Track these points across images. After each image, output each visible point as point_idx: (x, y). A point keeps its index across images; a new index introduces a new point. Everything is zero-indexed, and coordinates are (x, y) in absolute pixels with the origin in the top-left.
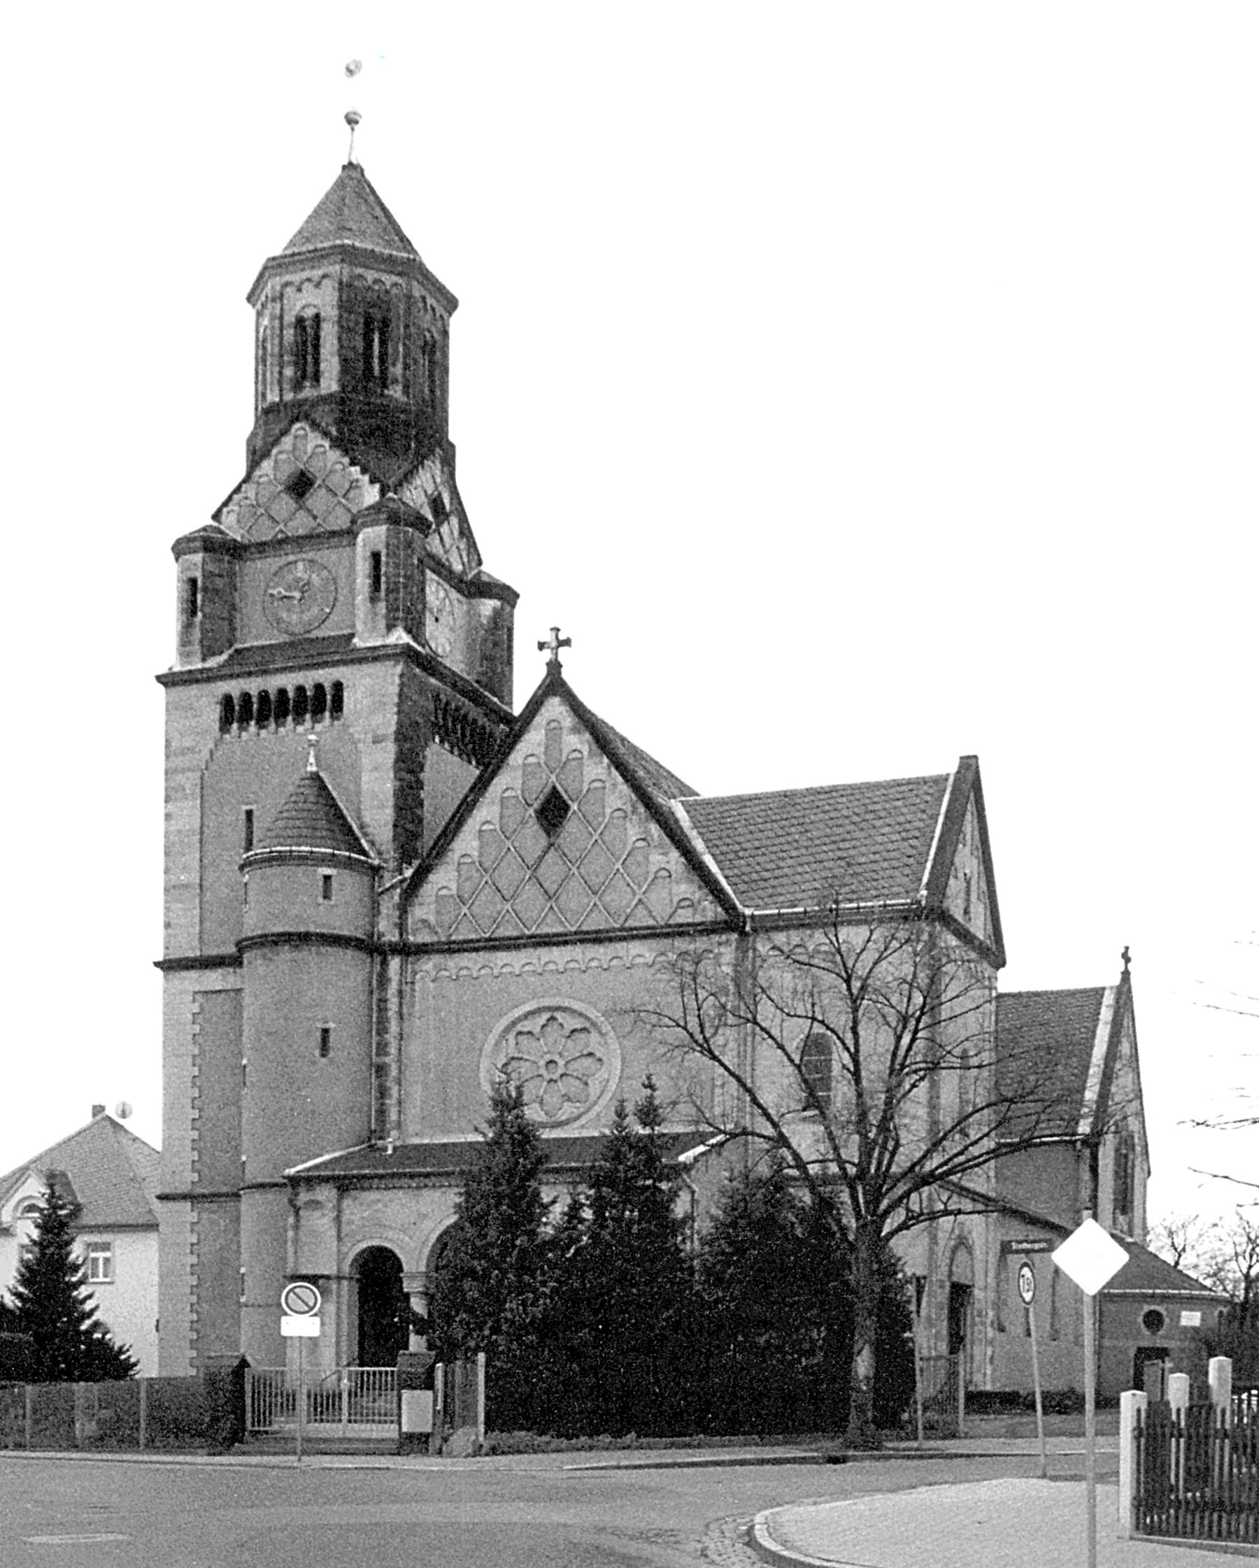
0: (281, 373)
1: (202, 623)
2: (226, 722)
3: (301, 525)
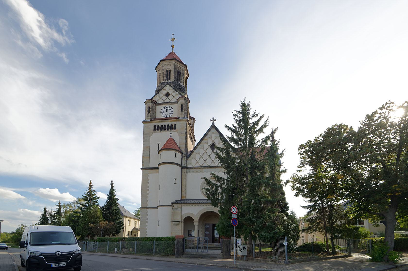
0: (164, 78)
1: (151, 114)
2: (155, 130)
3: (167, 101)
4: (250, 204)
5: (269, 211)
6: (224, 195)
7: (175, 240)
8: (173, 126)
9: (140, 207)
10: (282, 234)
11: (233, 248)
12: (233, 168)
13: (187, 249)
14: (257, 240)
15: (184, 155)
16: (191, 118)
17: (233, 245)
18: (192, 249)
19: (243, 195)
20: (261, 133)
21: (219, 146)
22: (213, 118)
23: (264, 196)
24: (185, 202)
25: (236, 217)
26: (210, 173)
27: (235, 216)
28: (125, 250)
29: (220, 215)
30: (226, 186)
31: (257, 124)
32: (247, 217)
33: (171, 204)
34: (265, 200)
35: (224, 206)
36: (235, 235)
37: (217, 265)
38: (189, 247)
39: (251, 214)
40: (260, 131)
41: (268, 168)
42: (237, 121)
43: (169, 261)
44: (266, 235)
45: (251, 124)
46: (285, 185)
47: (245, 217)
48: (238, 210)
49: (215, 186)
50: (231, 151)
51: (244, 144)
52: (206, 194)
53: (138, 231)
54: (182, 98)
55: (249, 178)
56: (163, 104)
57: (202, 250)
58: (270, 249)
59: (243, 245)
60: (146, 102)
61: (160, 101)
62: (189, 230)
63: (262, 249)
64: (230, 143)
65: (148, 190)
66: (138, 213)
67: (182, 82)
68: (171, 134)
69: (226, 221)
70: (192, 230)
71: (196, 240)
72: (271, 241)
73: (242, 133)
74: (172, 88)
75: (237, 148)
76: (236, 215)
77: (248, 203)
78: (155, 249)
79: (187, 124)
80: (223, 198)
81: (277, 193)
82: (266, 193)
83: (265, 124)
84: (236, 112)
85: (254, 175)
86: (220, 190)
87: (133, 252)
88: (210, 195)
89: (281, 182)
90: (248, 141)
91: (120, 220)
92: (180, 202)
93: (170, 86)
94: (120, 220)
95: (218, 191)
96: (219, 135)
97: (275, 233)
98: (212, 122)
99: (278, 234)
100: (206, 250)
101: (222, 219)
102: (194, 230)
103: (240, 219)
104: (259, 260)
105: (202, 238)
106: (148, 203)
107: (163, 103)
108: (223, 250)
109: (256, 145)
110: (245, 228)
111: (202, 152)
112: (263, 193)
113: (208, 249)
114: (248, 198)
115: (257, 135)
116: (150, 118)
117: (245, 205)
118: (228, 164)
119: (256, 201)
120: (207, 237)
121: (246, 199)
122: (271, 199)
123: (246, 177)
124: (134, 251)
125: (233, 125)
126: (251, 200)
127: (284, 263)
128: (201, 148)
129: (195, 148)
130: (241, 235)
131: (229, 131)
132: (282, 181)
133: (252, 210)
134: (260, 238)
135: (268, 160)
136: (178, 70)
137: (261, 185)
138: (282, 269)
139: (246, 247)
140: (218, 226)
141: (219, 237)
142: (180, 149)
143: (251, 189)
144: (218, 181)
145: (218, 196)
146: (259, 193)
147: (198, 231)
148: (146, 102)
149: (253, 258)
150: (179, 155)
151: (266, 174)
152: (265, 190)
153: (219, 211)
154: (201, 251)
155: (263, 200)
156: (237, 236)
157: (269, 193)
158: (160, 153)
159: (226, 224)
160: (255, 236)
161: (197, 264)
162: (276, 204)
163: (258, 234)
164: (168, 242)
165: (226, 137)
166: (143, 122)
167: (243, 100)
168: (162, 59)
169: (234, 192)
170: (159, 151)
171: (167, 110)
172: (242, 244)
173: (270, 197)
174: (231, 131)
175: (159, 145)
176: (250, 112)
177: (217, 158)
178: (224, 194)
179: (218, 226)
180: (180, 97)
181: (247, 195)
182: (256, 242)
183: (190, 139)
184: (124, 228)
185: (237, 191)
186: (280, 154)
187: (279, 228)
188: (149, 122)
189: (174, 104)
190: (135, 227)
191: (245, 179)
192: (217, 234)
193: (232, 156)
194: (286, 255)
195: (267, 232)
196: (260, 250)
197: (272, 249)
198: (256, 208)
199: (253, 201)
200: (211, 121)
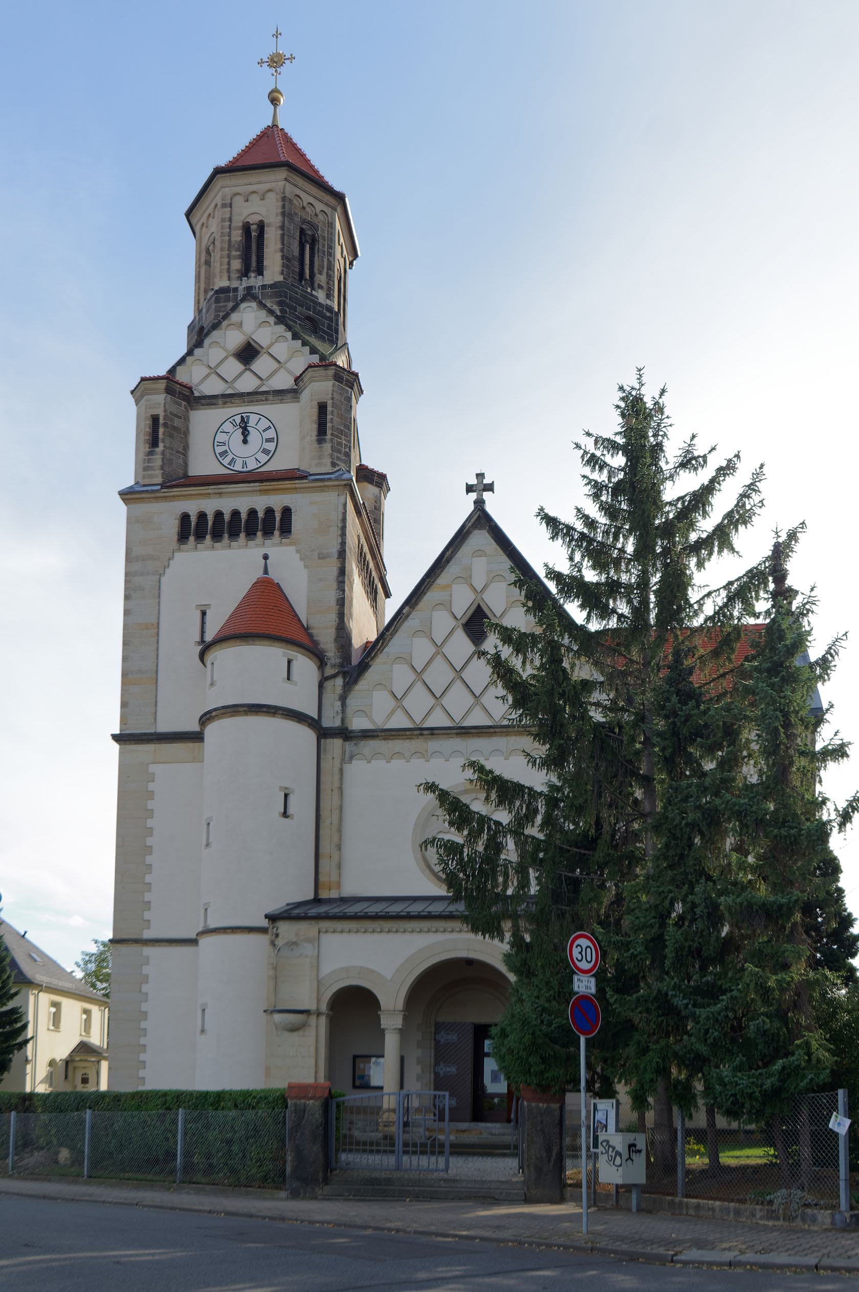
0: (229, 264)
1: (163, 453)
2: (183, 536)
3: (247, 384)
4: (663, 925)
5: (759, 957)
6: (532, 874)
7: (286, 1107)
8: (278, 516)
9: (111, 936)
10: (825, 1076)
11: (576, 1148)
12: (581, 733)
13: (344, 1151)
14: (696, 1106)
15: (334, 666)
16: (368, 476)
17: (576, 1134)
18: (371, 1152)
19: (626, 874)
20: (720, 551)
21: (507, 622)
22: (480, 476)
23: (735, 884)
24: (337, 910)
25: (593, 991)
26: (462, 761)
27: (584, 985)
28: (35, 1158)
29: (512, 977)
30: (541, 831)
31: (704, 505)
32: (649, 991)
33: (265, 923)
34: (738, 900)
35: (532, 933)
36: (587, 1081)
37: (494, 1236)
38: (358, 1143)
39: (667, 973)
40: (716, 543)
41: (753, 736)
42: (597, 489)
43: (257, 1217)
44: (744, 1081)
45: (670, 504)
46: (842, 825)
47: (636, 988)
48: (604, 954)
49: (489, 828)
50: (569, 649)
51: (635, 611)
52: (444, 870)
53: (99, 1062)
54: (321, 372)
55: (658, 787)
56: (225, 403)
57: (421, 1157)
58: (760, 1152)
59: (629, 1131)
60: (138, 393)
61: (212, 387)
62: (355, 1057)
63: (721, 1155)
64: (561, 607)
65: (149, 850)
66: (100, 967)
67: (320, 287)
68: (266, 557)
69: (544, 1010)
70: (370, 1057)
71: (393, 1105)
72: (768, 1110)
73: (625, 552)
74: (272, 320)
75: (597, 632)
76: (593, 980)
77: (655, 917)
78: (187, 1154)
79: (345, 505)
80: (524, 893)
81: (799, 863)
82: (742, 866)
83: (740, 505)
84: (596, 442)
85: (682, 773)
86: (510, 852)
87: (72, 1165)
88: (461, 875)
89: (822, 808)
90: (652, 598)
91: (11, 1005)
92: (313, 911)
93: (262, 305)
94: (11, 1005)
95: (503, 857)
96: (507, 563)
97: (786, 1074)
98: (473, 496)
99: (804, 1076)
100: (442, 1161)
101: (524, 997)
102: (383, 1056)
103: (612, 1001)
104: (709, 1209)
105: (419, 1096)
106: (147, 915)
107: (227, 398)
108: (526, 1156)
109: (696, 614)
110: (639, 1043)
111: (421, 650)
112: (729, 864)
113: (452, 1153)
114: (653, 890)
115: (700, 565)
116: (159, 472)
117: (637, 929)
118: (554, 717)
119: (694, 905)
120: (447, 1094)
121: (644, 898)
122: (772, 898)
123: (647, 781)
124: (81, 1164)
125: (579, 510)
126: (667, 902)
127: (833, 1223)
129: (386, 634)
130: (619, 1082)
131: (560, 541)
132: (829, 804)
133: (673, 955)
134: (715, 1098)
135: (754, 693)
136: (304, 221)
137: (719, 824)
138: (820, 1254)
139: (641, 1141)
140: (504, 1034)
141: (506, 1091)
142: (310, 636)
143: (667, 846)
144: (500, 803)
145: (501, 879)
146: (712, 865)
147: (402, 1059)
148: (138, 393)
149: (677, 1200)
150: (305, 667)
151: (745, 769)
152: (740, 849)
153: (507, 958)
154: (415, 1162)
155: (730, 900)
156: (597, 1085)
157: (761, 867)
158: (209, 658)
159: (544, 1027)
160: (687, 1086)
161: (398, 1231)
162: (795, 924)
163: (703, 1074)
164: (250, 1114)
165: (541, 573)
166: (127, 495)
167: (630, 381)
168: (223, 162)
169: (582, 861)
170: (205, 648)
171: (245, 433)
172: (621, 1126)
173: (763, 887)
174: (570, 541)
175: (204, 614)
176: (666, 443)
177: (500, 684)
178: (531, 870)
179: (504, 1034)
180: (310, 366)
181: (648, 877)
182: (691, 1117)
183: (363, 584)
184: (30, 1046)
185: (599, 855)
186: (816, 662)
187: (807, 1044)
188: (156, 498)
189: (281, 401)
190: (85, 1039)
191: (639, 794)
192: (495, 1078)
193: (576, 674)
194: (842, 1184)
195: (751, 1068)
196: (714, 1158)
197: (772, 1152)
198: (693, 941)
199: (679, 907)
200: (470, 489)
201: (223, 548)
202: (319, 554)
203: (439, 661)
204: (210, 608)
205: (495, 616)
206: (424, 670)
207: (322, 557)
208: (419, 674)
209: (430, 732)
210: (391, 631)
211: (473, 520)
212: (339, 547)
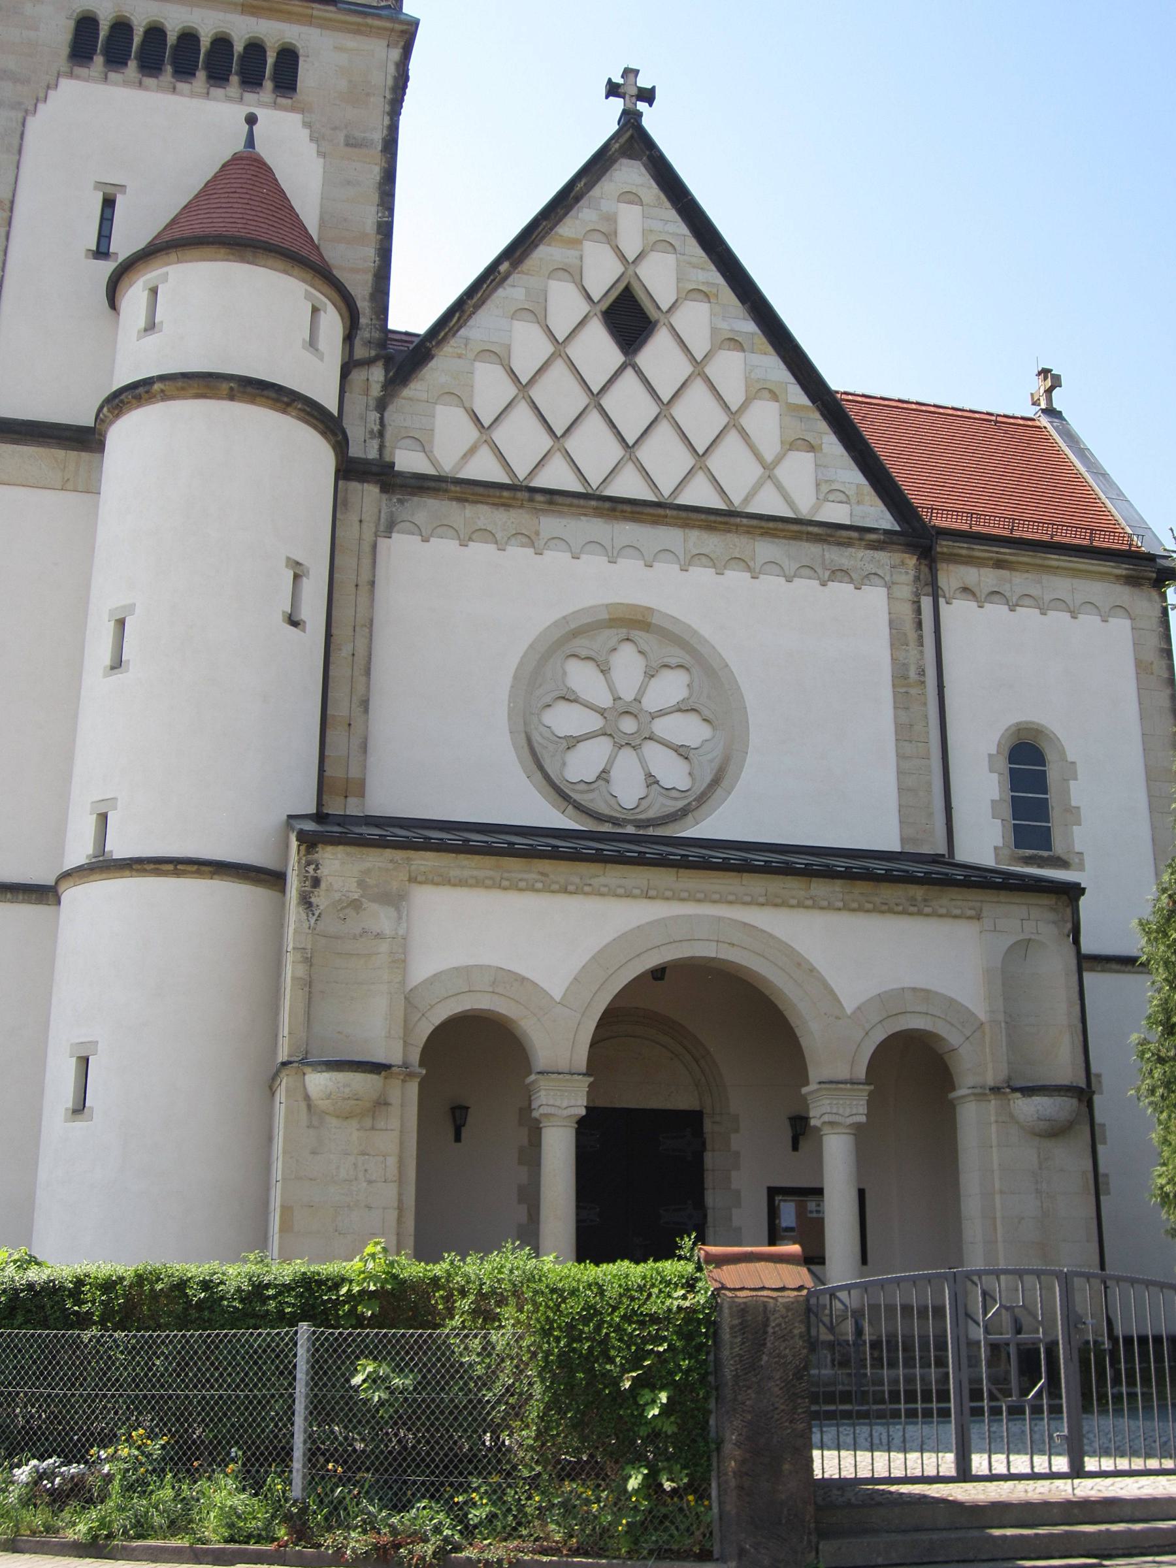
68: (251, 120)
98: (617, 105)
128: (519, 313)
200: (613, 90)
201: (160, 89)
202: (347, 137)
203: (559, 369)
204: (125, 193)
205: (659, 308)
206: (532, 381)
207: (352, 143)
208: (524, 388)
209: (548, 497)
210: (475, 300)
211: (622, 140)
212: (385, 132)
